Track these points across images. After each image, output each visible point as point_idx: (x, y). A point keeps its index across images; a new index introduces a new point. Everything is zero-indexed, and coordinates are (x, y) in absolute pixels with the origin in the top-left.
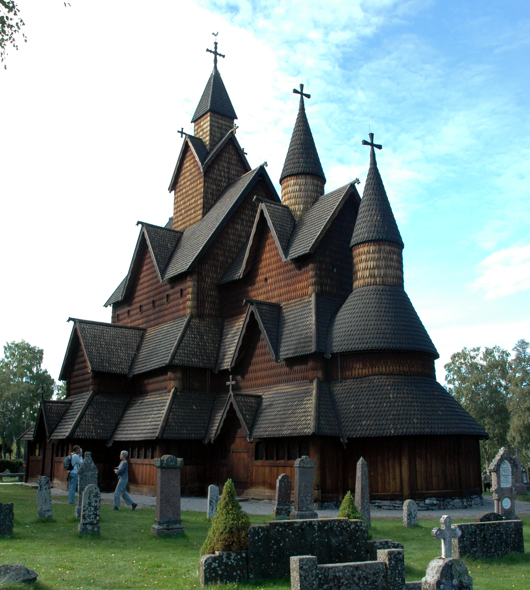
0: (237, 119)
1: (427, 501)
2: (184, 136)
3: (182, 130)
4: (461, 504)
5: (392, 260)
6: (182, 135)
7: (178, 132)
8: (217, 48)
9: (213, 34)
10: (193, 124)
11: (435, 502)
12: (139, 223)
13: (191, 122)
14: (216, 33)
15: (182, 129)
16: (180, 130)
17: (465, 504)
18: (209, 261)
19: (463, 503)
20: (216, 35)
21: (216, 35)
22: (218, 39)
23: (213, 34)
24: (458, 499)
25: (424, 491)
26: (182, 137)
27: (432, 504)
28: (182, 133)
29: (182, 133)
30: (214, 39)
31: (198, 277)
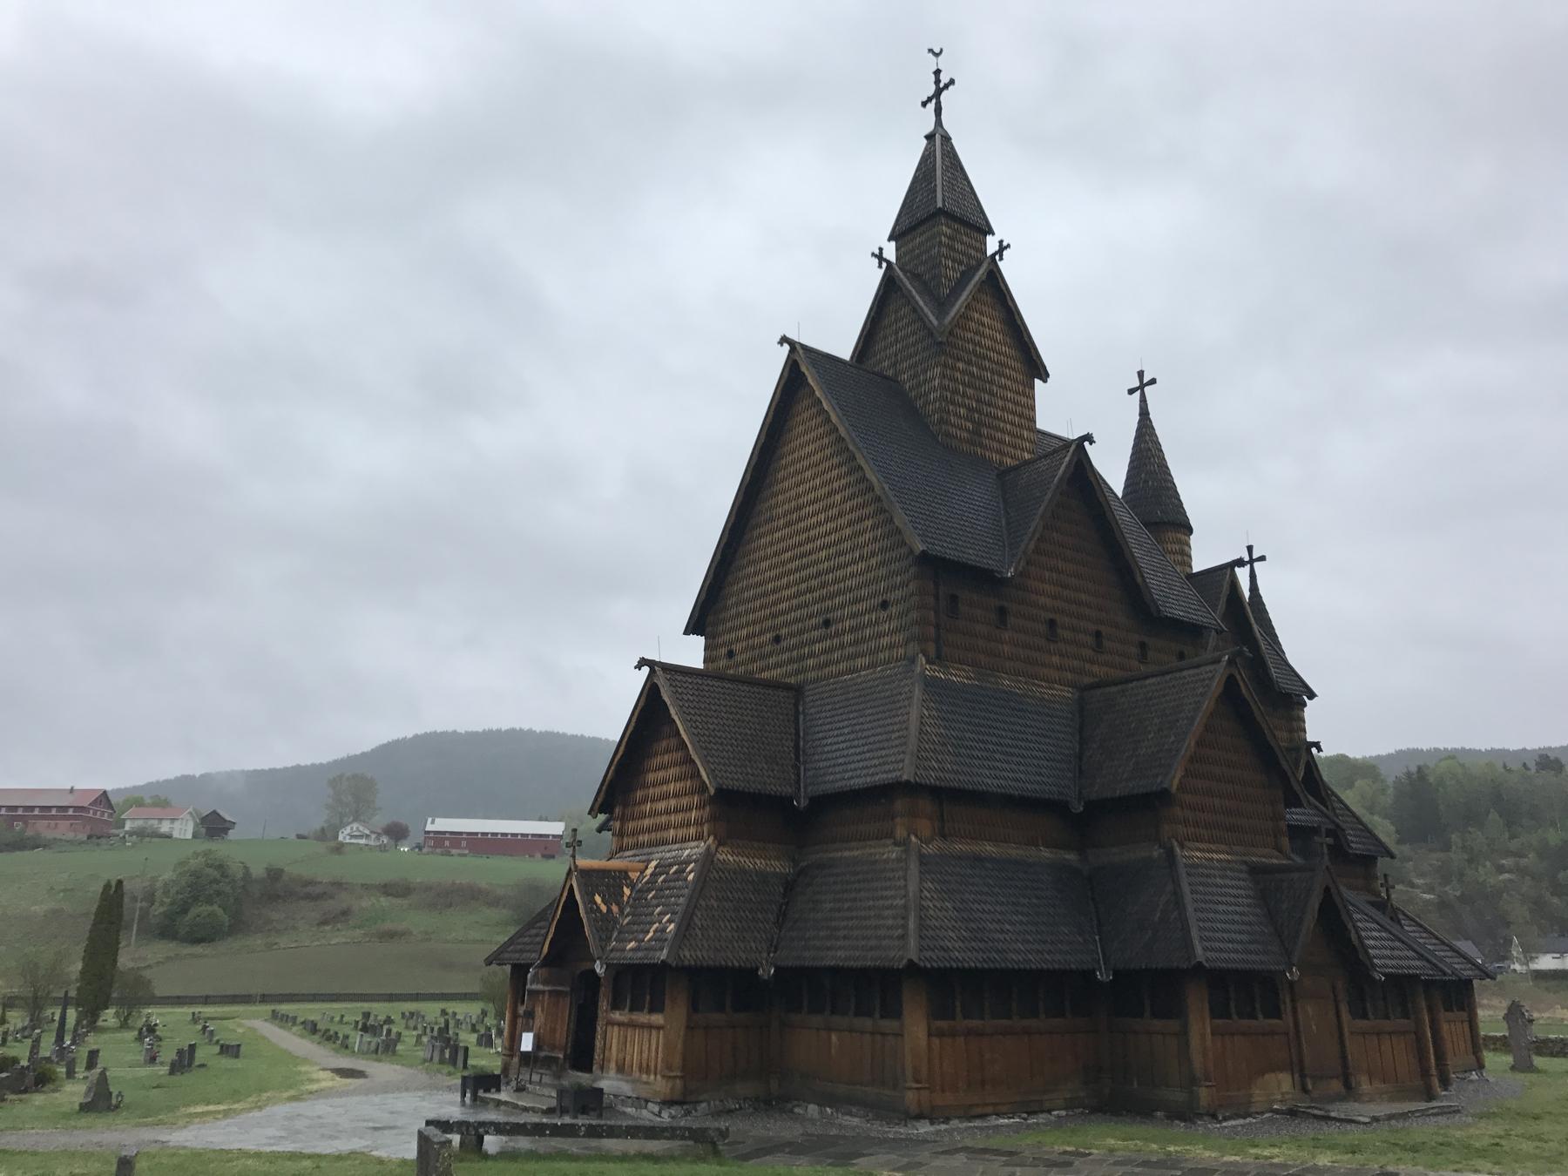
0: (993, 234)
2: (884, 265)
7: (873, 254)
8: (935, 83)
9: (931, 51)
10: (893, 244)
14: (937, 50)
16: (877, 252)
20: (937, 55)
21: (937, 55)
22: (942, 62)
23: (931, 51)
26: (880, 266)
28: (880, 257)
29: (880, 257)
30: (931, 63)
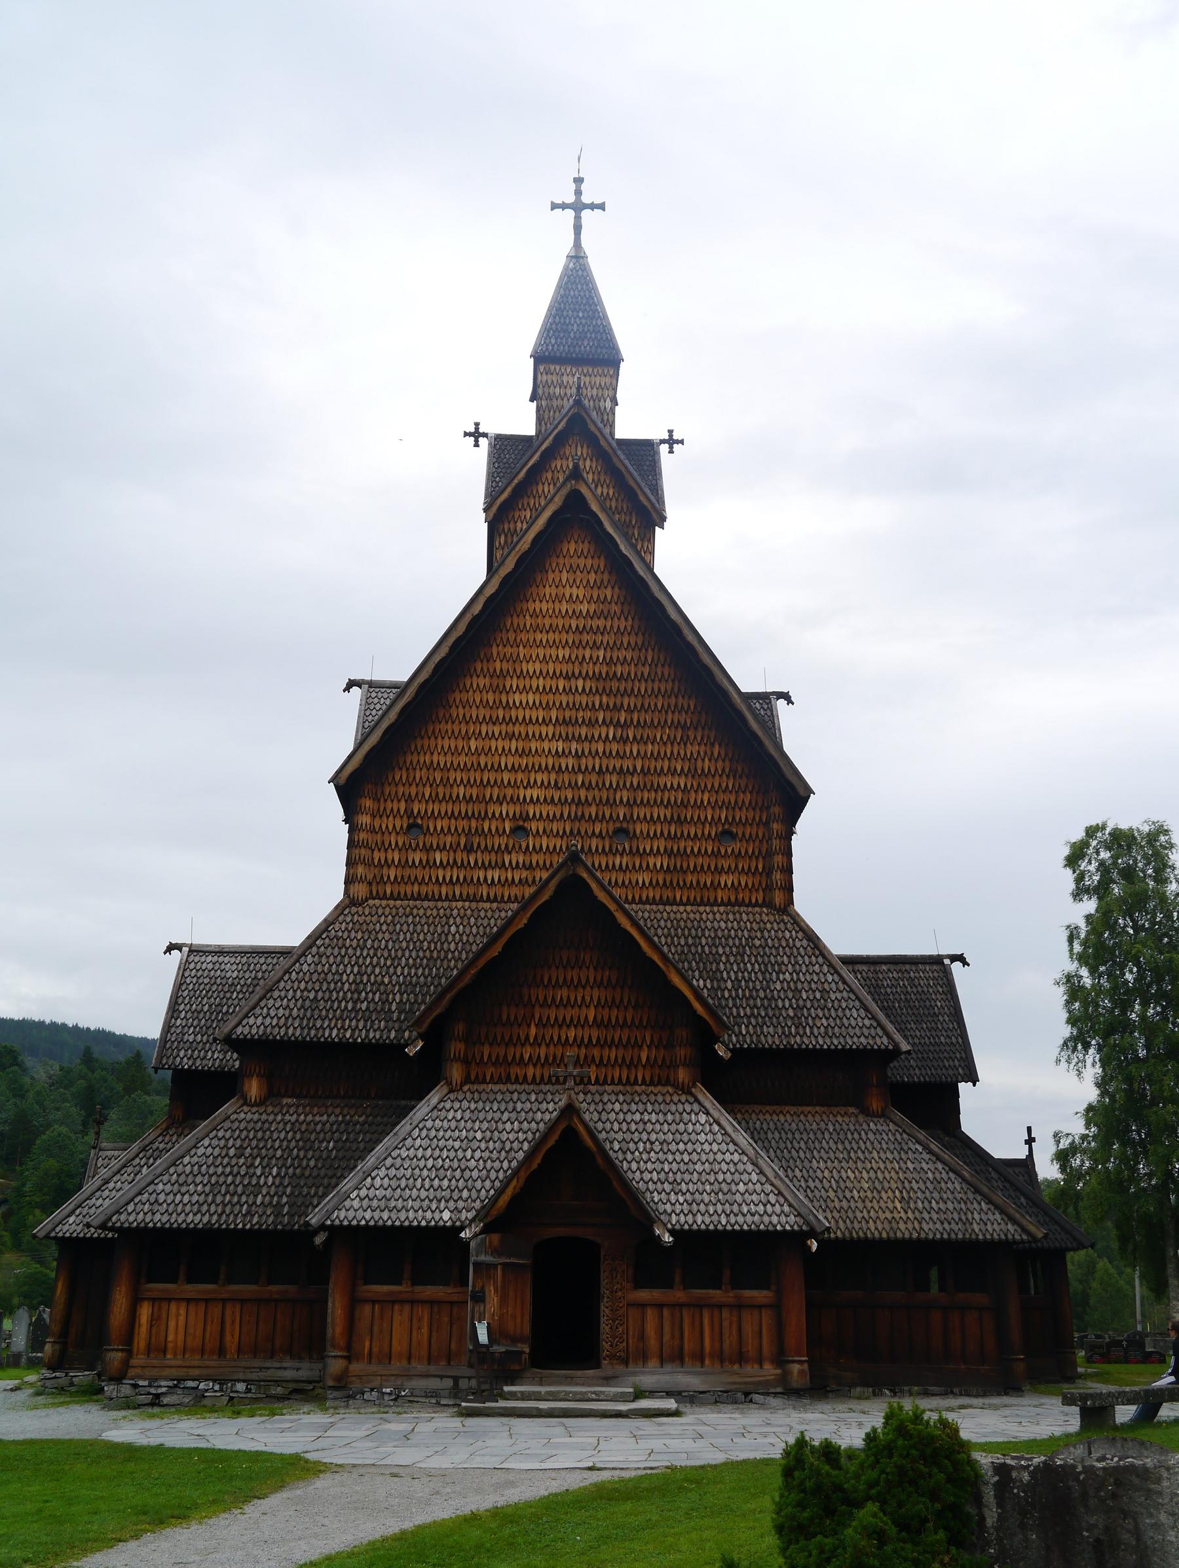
2: (483, 442)
3: (477, 429)
7: (466, 434)
12: (351, 684)
13: (532, 400)
15: (477, 424)
26: (477, 445)
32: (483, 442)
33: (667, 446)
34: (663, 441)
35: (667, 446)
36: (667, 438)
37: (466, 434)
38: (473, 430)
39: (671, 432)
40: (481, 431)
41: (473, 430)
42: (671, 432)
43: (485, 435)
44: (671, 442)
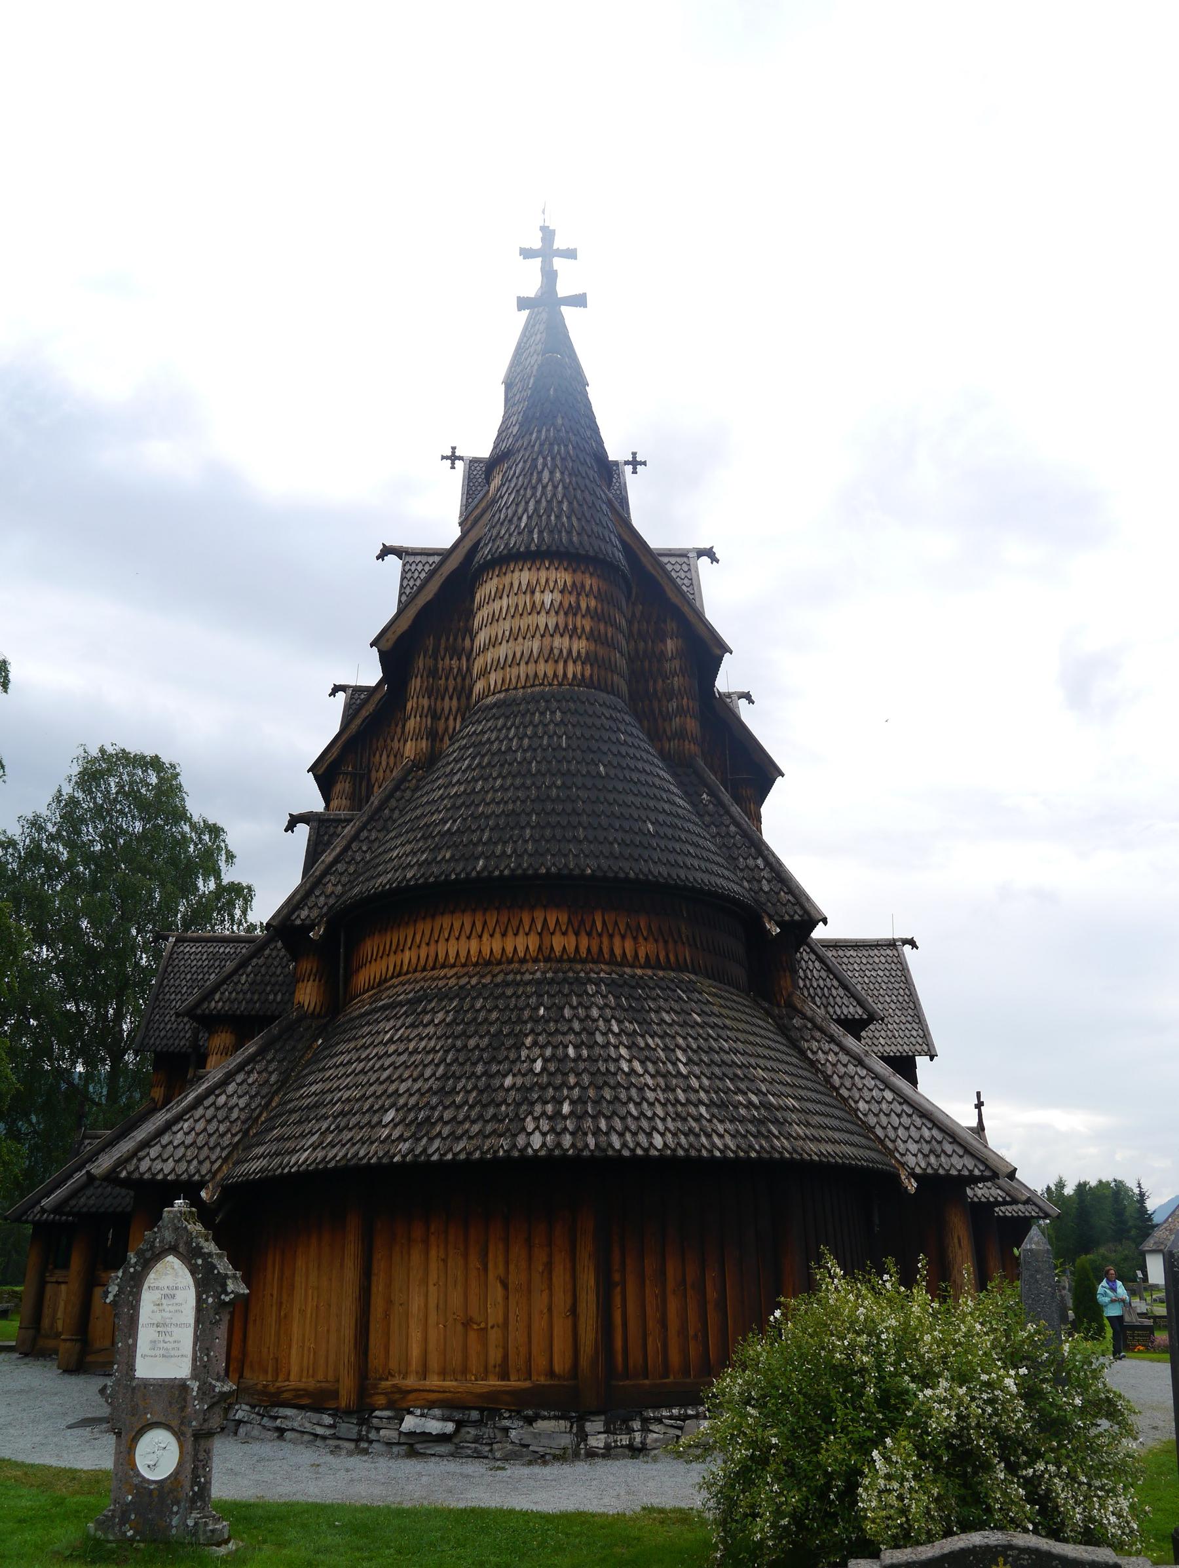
1: (410, 1423)
3: (453, 452)
4: (566, 1440)
5: (535, 609)
6: (453, 463)
7: (443, 458)
11: (434, 1426)
12: (336, 689)
15: (454, 448)
17: (597, 1442)
18: (392, 741)
19: (583, 1436)
24: (557, 1418)
25: (411, 1382)
26: (453, 467)
27: (423, 1433)
28: (453, 458)
31: (354, 784)
32: (459, 464)
33: (631, 467)
34: (627, 463)
35: (631, 467)
36: (631, 459)
37: (443, 458)
38: (450, 454)
39: (634, 454)
40: (457, 454)
41: (450, 454)
42: (634, 454)
43: (460, 458)
44: (635, 463)
